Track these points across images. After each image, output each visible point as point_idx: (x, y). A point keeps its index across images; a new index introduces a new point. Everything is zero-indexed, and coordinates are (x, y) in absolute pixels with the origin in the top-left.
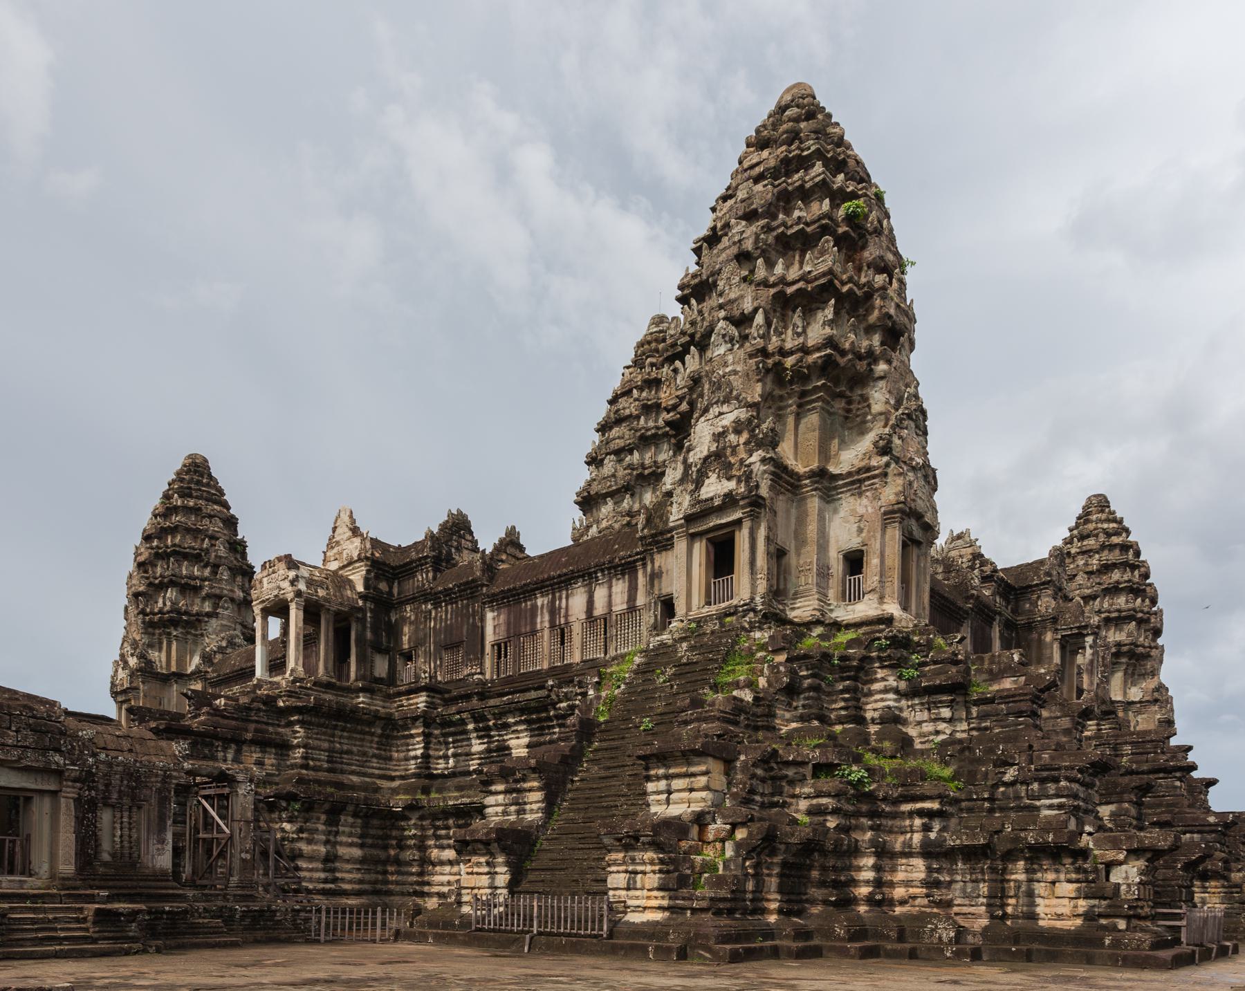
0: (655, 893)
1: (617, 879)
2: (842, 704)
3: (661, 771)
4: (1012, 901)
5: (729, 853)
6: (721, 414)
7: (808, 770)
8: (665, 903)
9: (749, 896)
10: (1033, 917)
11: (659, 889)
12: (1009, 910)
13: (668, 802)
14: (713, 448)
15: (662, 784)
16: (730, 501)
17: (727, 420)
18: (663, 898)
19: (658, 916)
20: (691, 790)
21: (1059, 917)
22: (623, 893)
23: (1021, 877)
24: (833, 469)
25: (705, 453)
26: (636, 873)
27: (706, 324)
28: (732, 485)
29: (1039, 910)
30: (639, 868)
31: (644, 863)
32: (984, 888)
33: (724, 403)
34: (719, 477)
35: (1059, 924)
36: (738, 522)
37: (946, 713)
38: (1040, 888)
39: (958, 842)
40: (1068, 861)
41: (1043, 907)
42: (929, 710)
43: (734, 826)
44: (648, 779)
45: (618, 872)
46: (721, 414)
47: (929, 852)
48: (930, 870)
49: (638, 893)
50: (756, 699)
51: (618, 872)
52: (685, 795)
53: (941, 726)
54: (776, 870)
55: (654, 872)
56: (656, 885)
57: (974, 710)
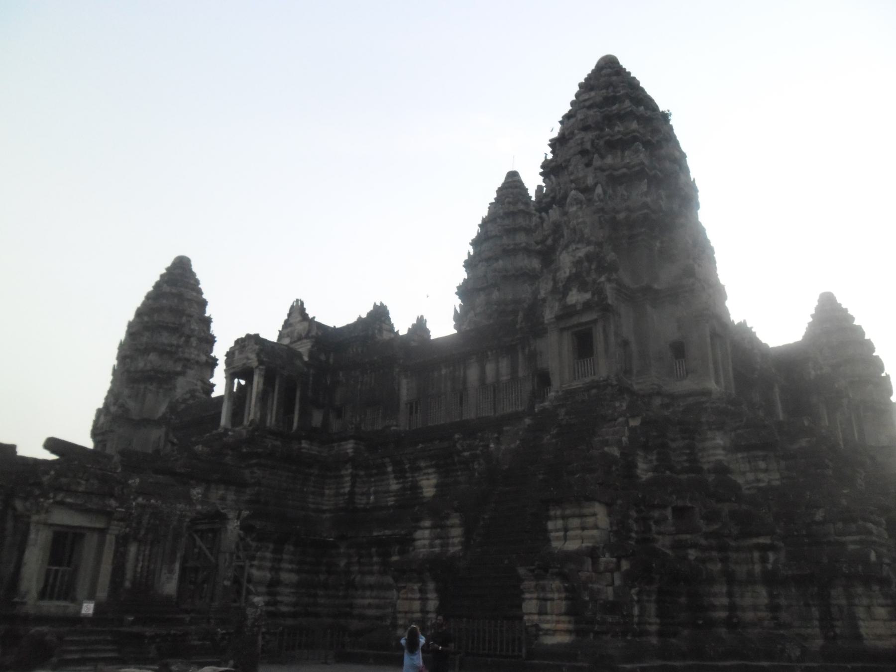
0: (563, 618)
1: (530, 605)
2: (685, 458)
3: (559, 512)
4: (839, 623)
5: (618, 582)
6: (577, 249)
7: (669, 512)
8: (571, 627)
9: (636, 620)
10: (859, 637)
11: (567, 614)
12: (838, 631)
13: (565, 538)
14: (574, 271)
15: (560, 523)
16: (587, 306)
17: (581, 254)
18: (569, 622)
19: (565, 639)
20: (583, 528)
21: (879, 637)
22: (536, 617)
23: (843, 602)
24: (656, 286)
25: (568, 274)
26: (546, 600)
27: (562, 191)
28: (588, 296)
29: (863, 631)
30: (550, 595)
31: (552, 591)
32: (815, 612)
33: (578, 242)
34: (579, 291)
35: (879, 644)
36: (595, 321)
37: (762, 465)
38: (861, 613)
39: (790, 572)
40: (876, 588)
41: (865, 628)
42: (749, 462)
43: (619, 559)
44: (549, 518)
45: (530, 599)
46: (577, 249)
47: (771, 579)
48: (771, 596)
49: (549, 618)
50: (622, 454)
51: (530, 599)
52: (579, 532)
53: (761, 476)
54: (654, 597)
55: (560, 599)
56: (563, 610)
57: (783, 463)
